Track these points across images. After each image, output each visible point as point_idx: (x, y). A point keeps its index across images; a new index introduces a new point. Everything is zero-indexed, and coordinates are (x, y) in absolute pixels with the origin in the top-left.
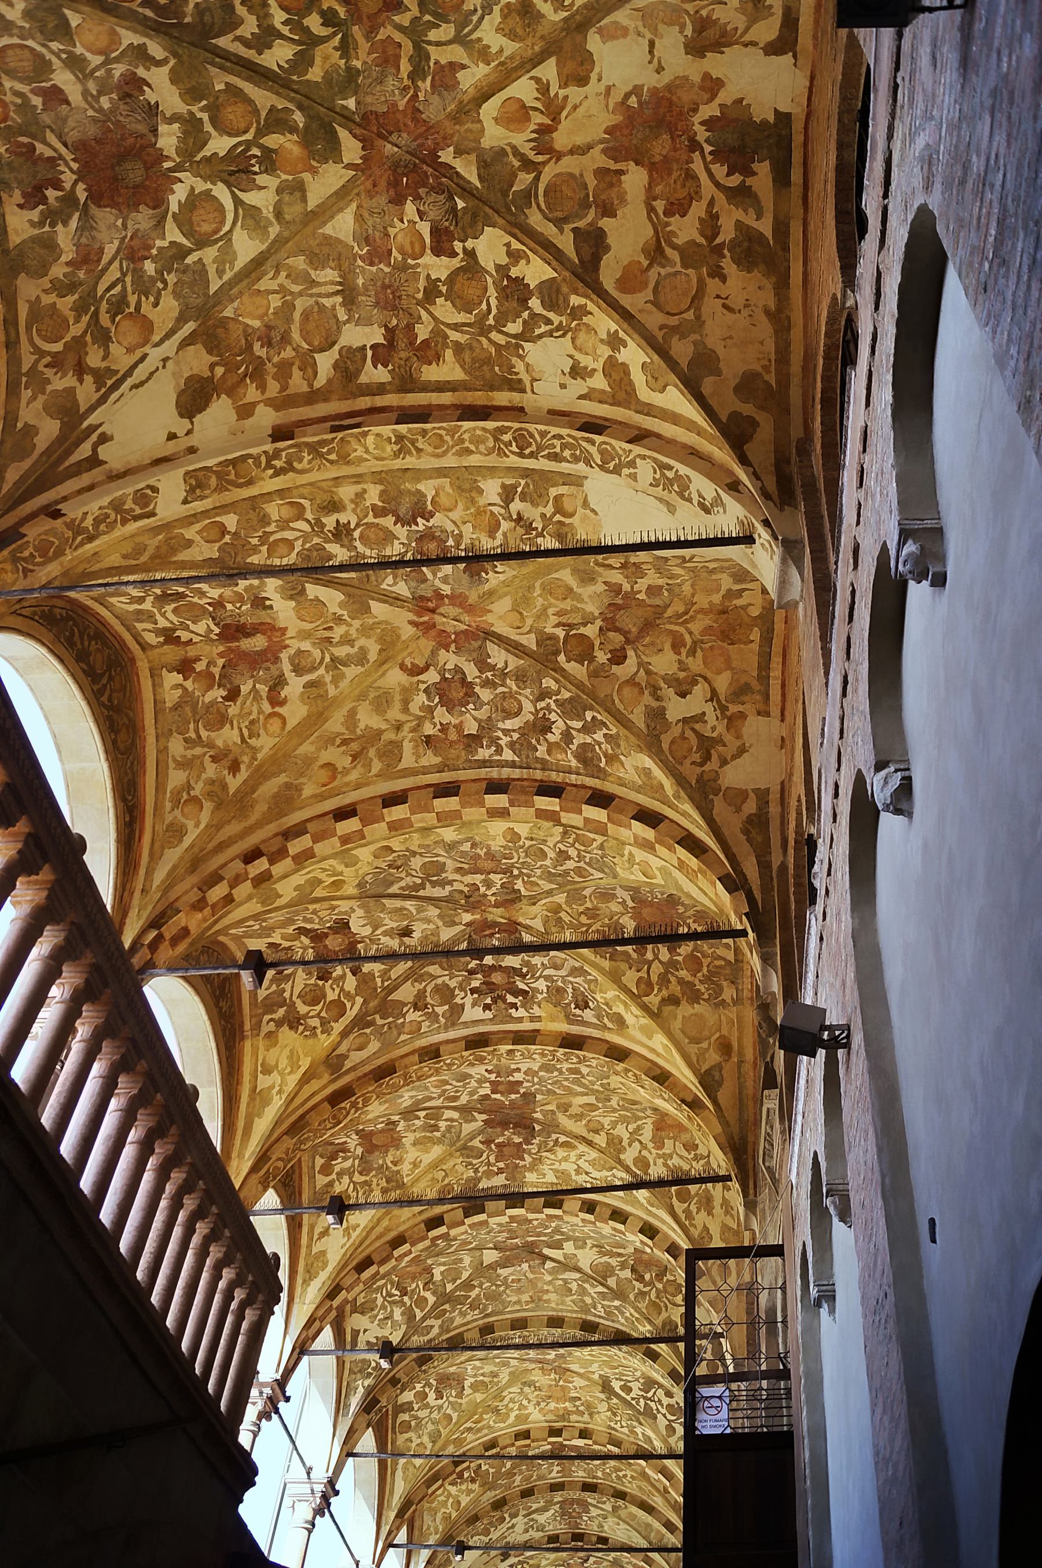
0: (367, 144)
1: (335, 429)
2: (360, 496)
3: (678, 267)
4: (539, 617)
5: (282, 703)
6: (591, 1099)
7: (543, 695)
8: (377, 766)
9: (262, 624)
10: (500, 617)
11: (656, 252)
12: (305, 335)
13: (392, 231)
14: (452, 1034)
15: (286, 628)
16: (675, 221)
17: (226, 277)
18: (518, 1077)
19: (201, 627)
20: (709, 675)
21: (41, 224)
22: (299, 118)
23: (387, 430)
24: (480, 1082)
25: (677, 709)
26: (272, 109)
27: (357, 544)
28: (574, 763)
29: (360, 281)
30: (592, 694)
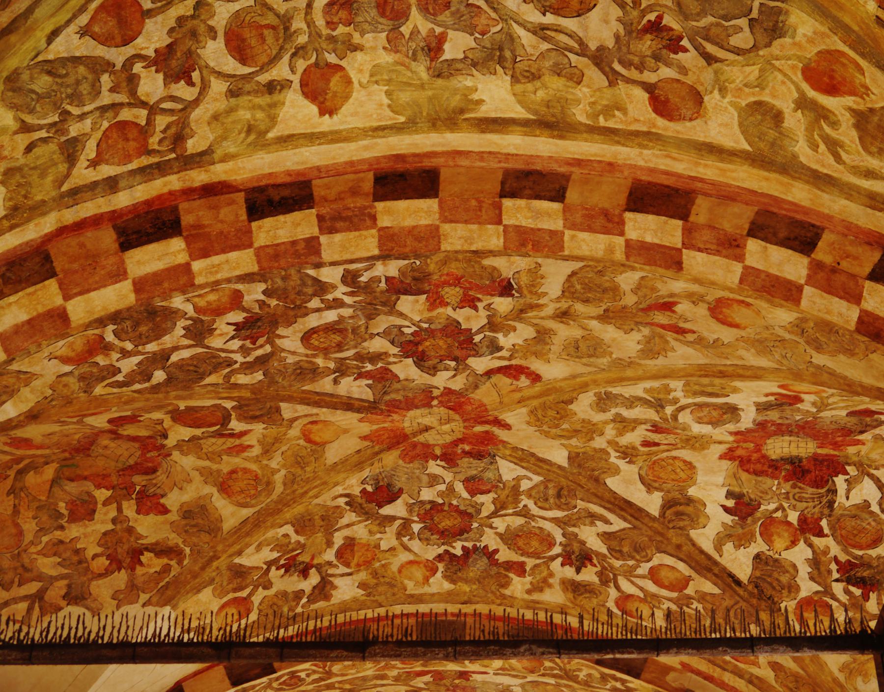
2: (537, 588)
4: (277, 440)
9: (757, 473)
10: (346, 431)
15: (721, 457)
27: (559, 538)
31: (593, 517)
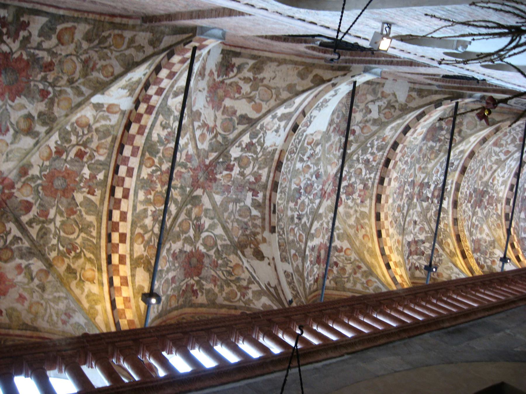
0: (198, 187)
1: (274, 212)
2: (292, 210)
3: (257, 93)
5: (342, 248)
6: (481, 167)
7: (358, 160)
8: (366, 221)
11: (250, 99)
12: (245, 217)
13: (223, 183)
14: (450, 213)
16: (243, 91)
17: (226, 238)
18: (468, 193)
19: (315, 270)
20: (366, 102)
21: (202, 292)
22: (189, 206)
23: (278, 196)
24: (467, 206)
25: (375, 114)
26: (186, 214)
28: (381, 153)
29: (234, 196)
30: (363, 143)
31: (308, 219)
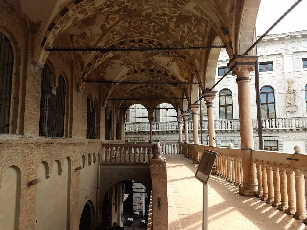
22: (151, 18)
29: (144, 2)
